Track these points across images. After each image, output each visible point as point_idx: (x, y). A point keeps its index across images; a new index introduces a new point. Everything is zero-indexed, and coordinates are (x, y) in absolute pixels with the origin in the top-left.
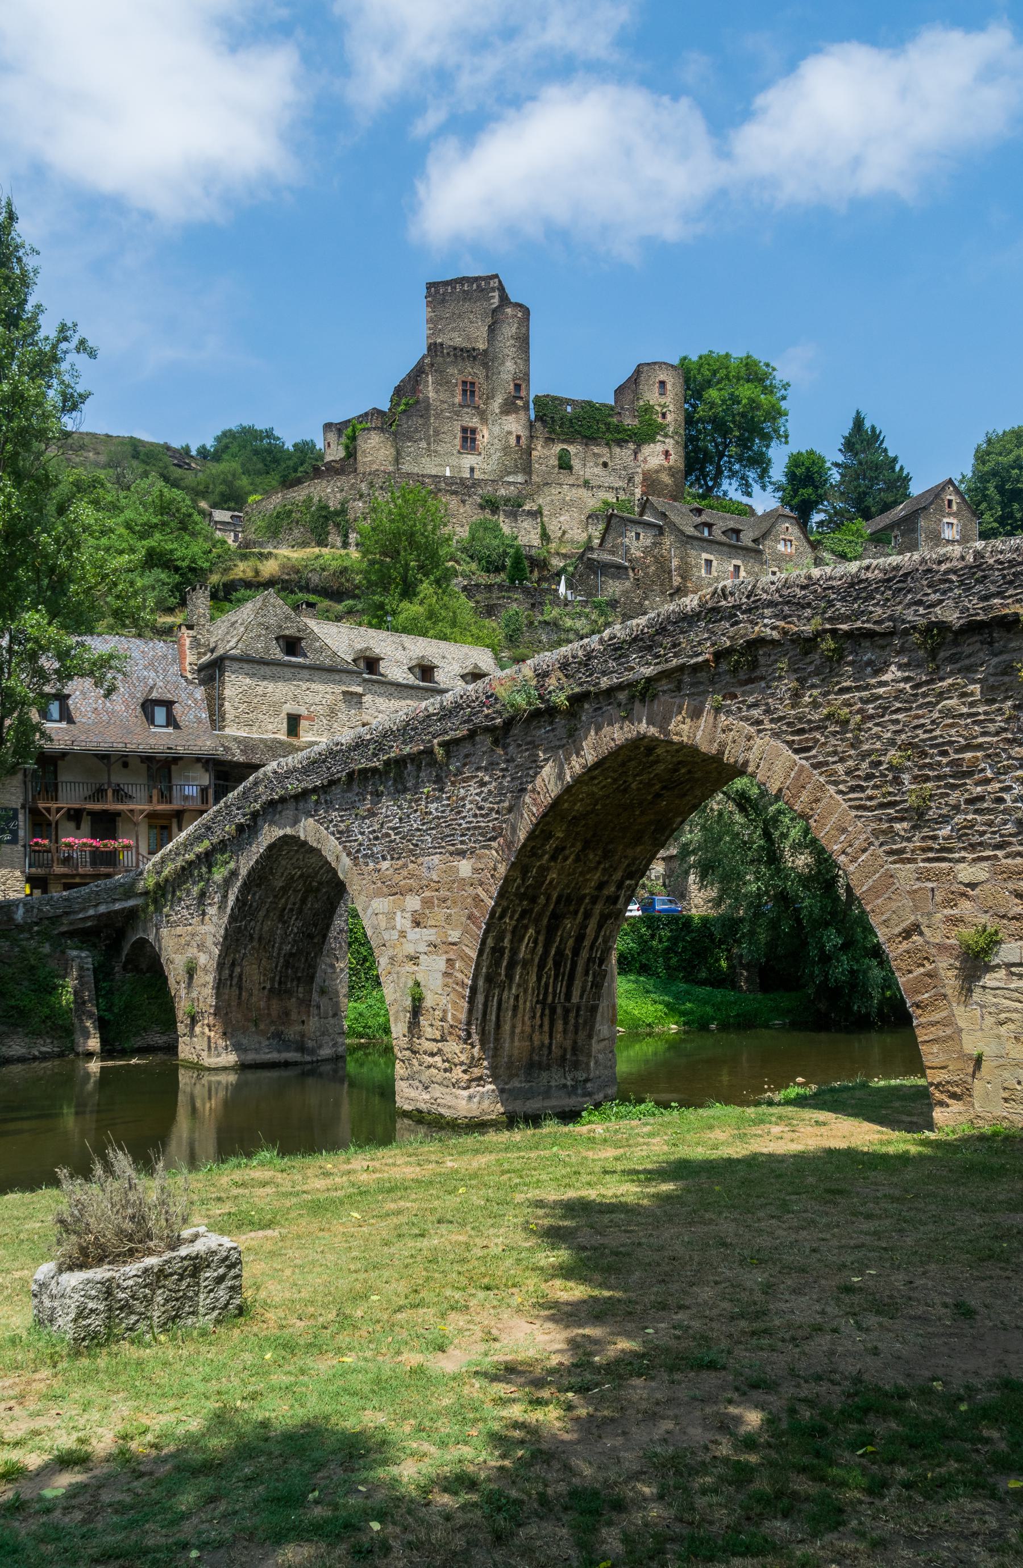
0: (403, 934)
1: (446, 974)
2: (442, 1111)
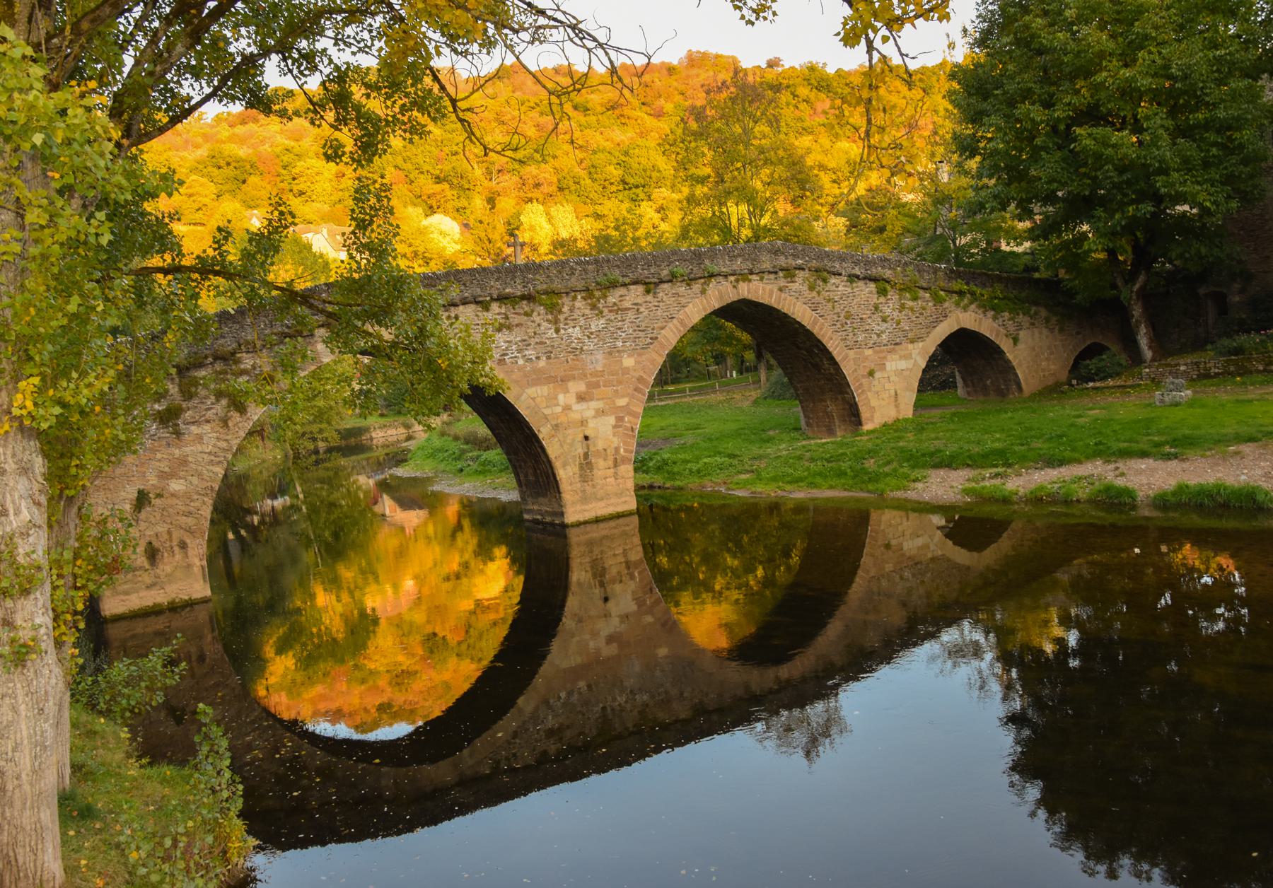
0: (567, 408)
1: (615, 427)
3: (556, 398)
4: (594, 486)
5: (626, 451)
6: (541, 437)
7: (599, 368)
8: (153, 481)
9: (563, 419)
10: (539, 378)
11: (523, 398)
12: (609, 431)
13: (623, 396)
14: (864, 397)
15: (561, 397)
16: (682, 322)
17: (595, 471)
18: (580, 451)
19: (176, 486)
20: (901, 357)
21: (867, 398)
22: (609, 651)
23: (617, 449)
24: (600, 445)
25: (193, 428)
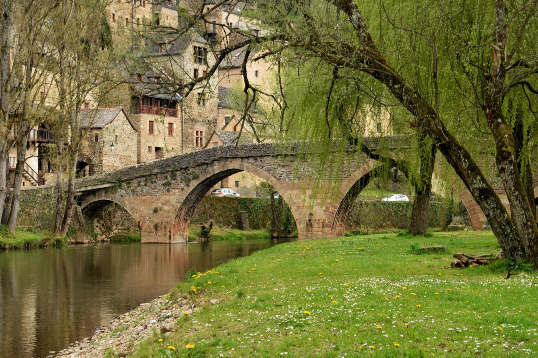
1: (324, 211)
5: (328, 221)
8: (160, 205)
9: (302, 205)
10: (294, 187)
14: (475, 216)
16: (364, 169)
17: (313, 228)
18: (308, 218)
19: (166, 208)
21: (478, 216)
23: (324, 220)
24: (317, 218)
25: (173, 190)
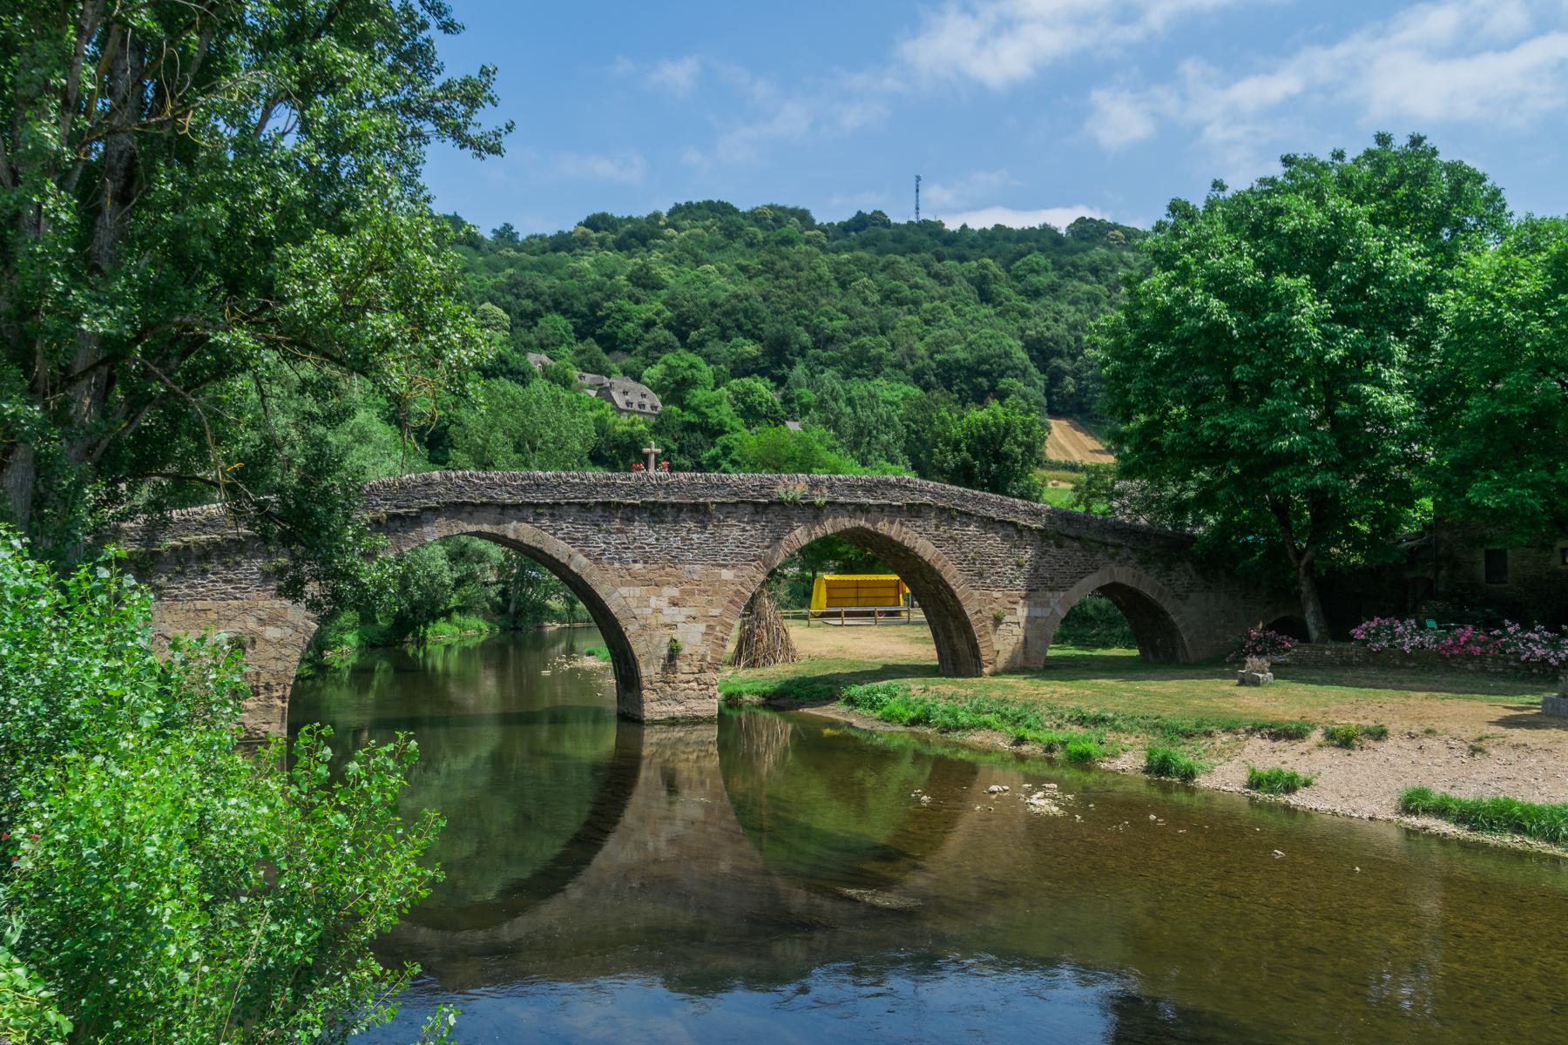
2: (699, 714)
3: (647, 600)
4: (674, 689)
6: (627, 634)
7: (696, 577)
11: (616, 595)
12: (699, 638)
13: (717, 607)
15: (653, 601)
20: (1036, 604)
22: (667, 852)
